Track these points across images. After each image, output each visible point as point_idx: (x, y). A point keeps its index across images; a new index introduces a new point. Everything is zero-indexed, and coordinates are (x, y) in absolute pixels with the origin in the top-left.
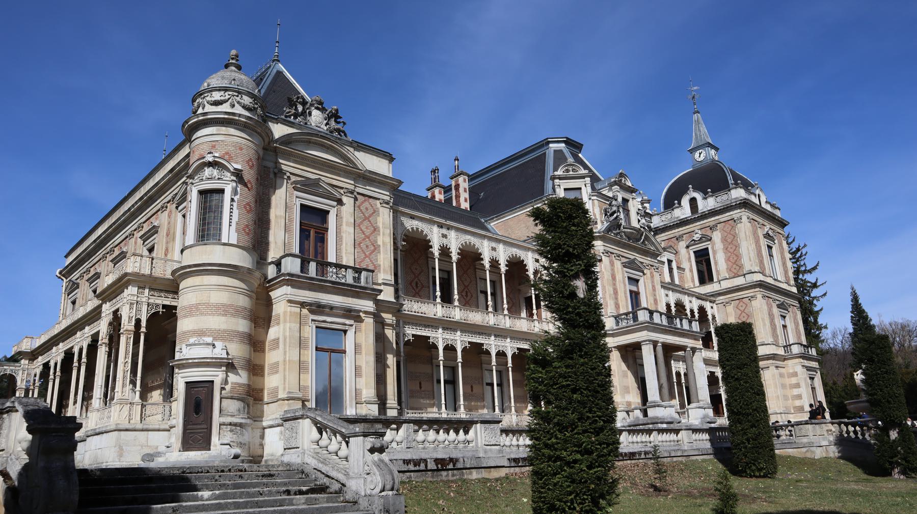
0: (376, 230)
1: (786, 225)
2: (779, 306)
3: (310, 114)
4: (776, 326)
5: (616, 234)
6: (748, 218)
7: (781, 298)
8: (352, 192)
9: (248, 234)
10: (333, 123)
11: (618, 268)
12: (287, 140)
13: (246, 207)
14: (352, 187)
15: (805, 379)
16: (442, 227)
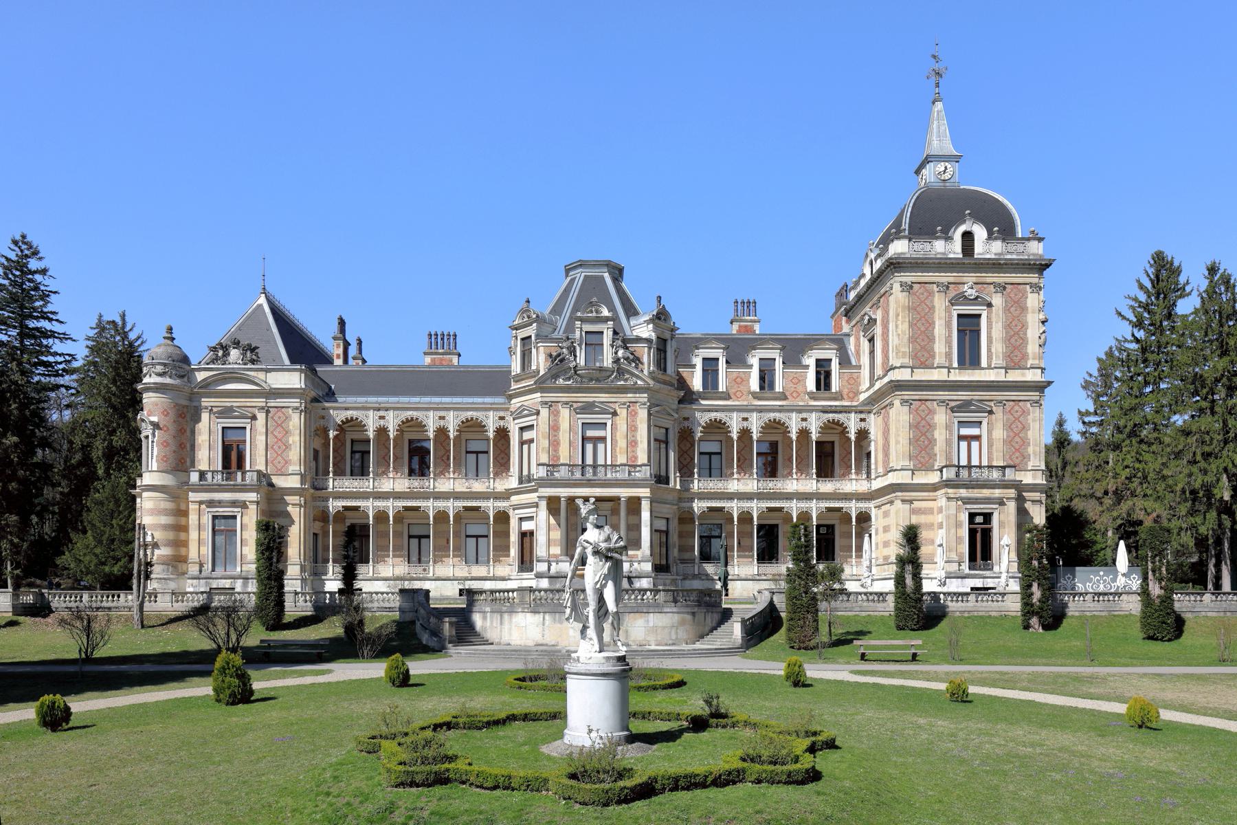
0: (287, 432)
1: (1048, 266)
2: (952, 410)
3: (229, 354)
4: (932, 442)
5: (569, 379)
6: (901, 286)
7: (964, 395)
8: (263, 408)
9: (166, 461)
10: (248, 353)
11: (563, 417)
12: (206, 384)
13: (165, 444)
14: (264, 404)
15: (948, 517)
16: (379, 410)
